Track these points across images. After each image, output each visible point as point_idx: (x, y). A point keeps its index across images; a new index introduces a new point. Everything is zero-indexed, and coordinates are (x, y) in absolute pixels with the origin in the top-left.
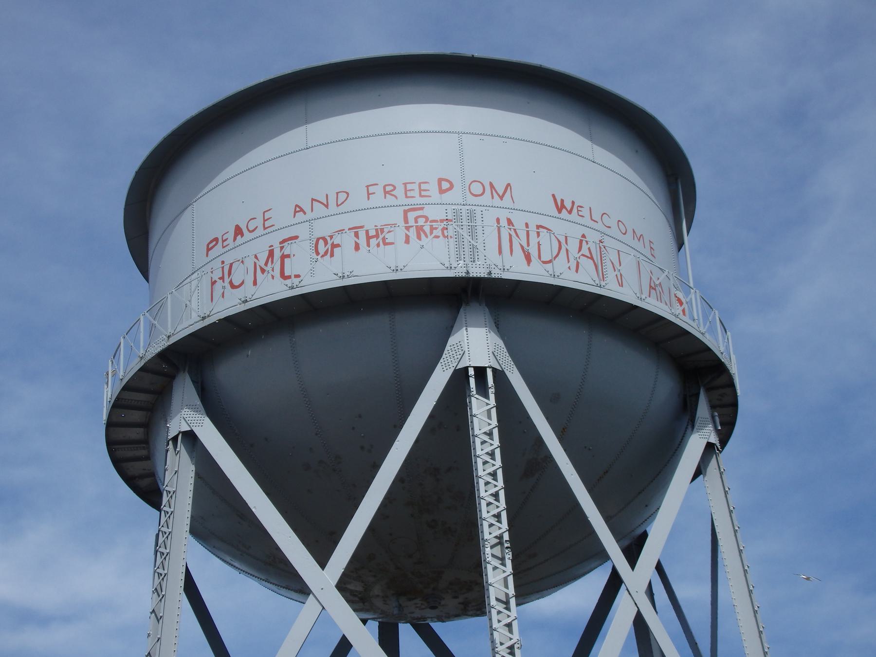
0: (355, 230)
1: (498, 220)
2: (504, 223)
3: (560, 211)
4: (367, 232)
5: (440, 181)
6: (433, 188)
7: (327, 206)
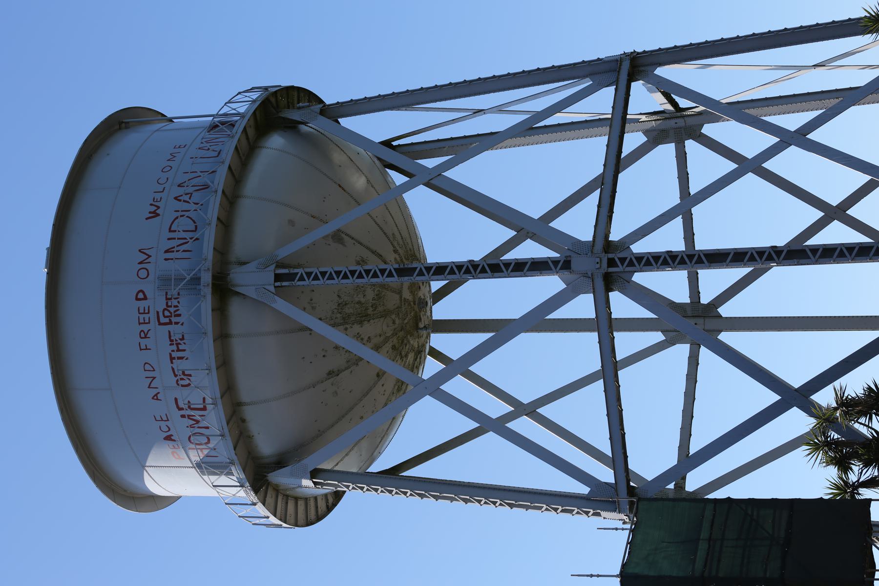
0: (172, 359)
1: (166, 259)
3: (158, 215)
4: (173, 351)
5: (137, 299)
6: (143, 304)
7: (154, 378)
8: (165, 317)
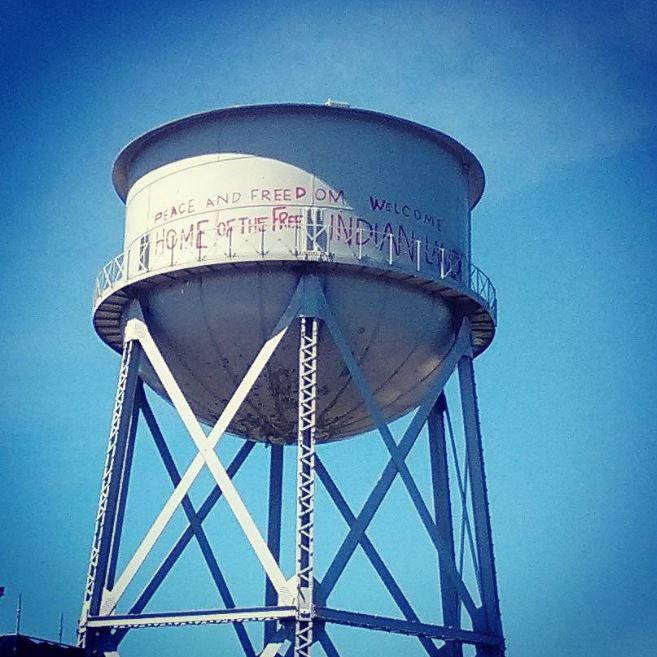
0: (243, 219)
1: (332, 216)
2: (336, 218)
3: (374, 208)
8: (280, 215)
